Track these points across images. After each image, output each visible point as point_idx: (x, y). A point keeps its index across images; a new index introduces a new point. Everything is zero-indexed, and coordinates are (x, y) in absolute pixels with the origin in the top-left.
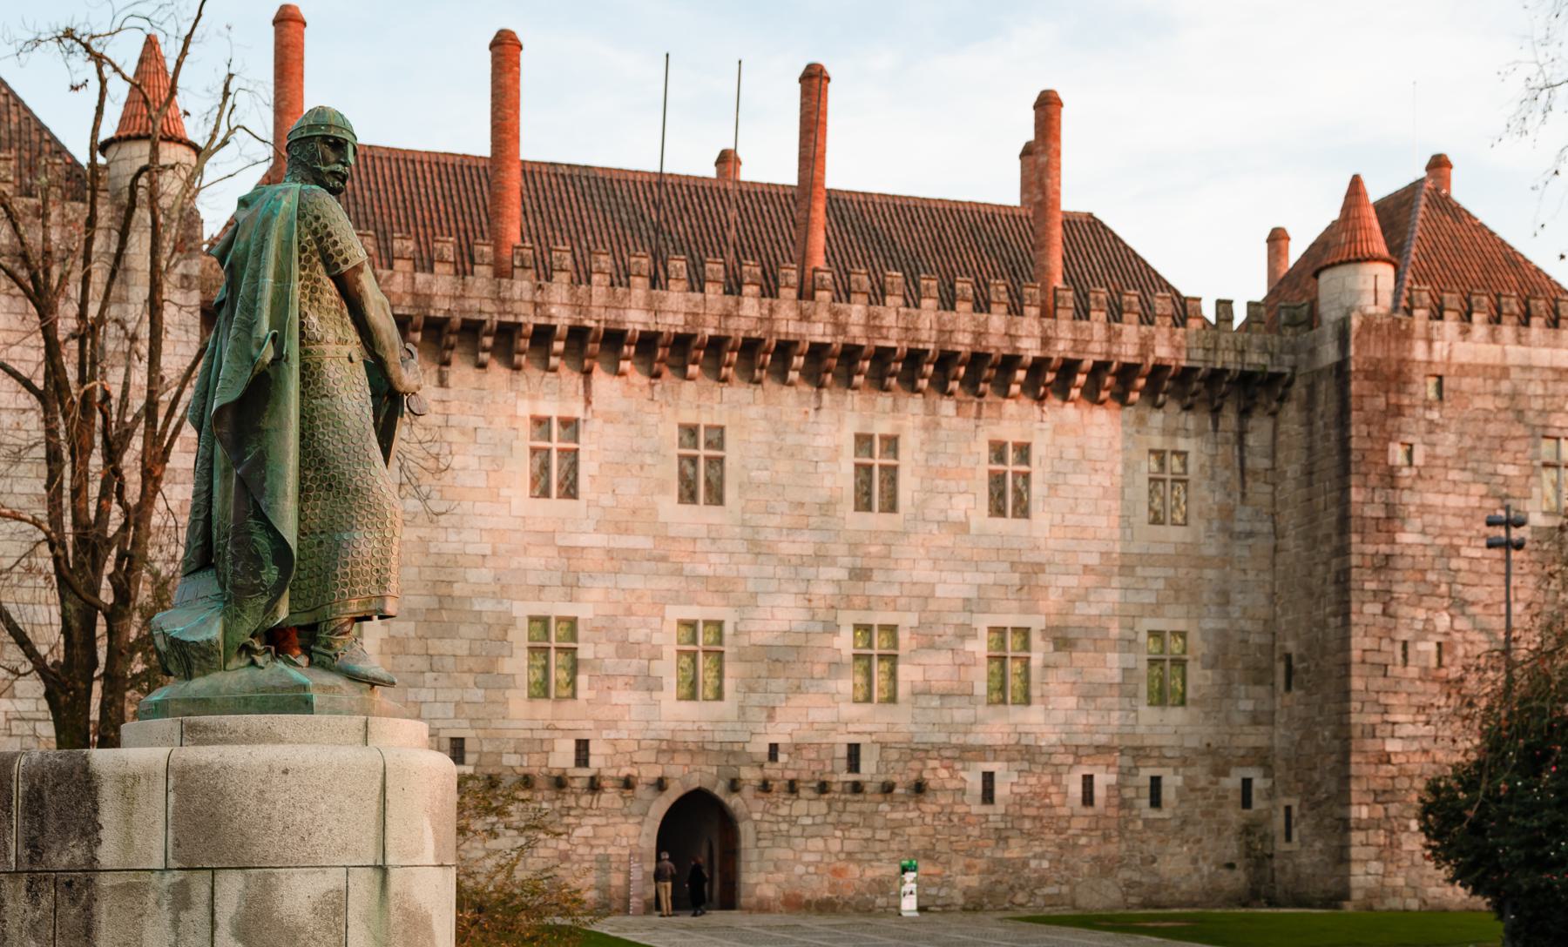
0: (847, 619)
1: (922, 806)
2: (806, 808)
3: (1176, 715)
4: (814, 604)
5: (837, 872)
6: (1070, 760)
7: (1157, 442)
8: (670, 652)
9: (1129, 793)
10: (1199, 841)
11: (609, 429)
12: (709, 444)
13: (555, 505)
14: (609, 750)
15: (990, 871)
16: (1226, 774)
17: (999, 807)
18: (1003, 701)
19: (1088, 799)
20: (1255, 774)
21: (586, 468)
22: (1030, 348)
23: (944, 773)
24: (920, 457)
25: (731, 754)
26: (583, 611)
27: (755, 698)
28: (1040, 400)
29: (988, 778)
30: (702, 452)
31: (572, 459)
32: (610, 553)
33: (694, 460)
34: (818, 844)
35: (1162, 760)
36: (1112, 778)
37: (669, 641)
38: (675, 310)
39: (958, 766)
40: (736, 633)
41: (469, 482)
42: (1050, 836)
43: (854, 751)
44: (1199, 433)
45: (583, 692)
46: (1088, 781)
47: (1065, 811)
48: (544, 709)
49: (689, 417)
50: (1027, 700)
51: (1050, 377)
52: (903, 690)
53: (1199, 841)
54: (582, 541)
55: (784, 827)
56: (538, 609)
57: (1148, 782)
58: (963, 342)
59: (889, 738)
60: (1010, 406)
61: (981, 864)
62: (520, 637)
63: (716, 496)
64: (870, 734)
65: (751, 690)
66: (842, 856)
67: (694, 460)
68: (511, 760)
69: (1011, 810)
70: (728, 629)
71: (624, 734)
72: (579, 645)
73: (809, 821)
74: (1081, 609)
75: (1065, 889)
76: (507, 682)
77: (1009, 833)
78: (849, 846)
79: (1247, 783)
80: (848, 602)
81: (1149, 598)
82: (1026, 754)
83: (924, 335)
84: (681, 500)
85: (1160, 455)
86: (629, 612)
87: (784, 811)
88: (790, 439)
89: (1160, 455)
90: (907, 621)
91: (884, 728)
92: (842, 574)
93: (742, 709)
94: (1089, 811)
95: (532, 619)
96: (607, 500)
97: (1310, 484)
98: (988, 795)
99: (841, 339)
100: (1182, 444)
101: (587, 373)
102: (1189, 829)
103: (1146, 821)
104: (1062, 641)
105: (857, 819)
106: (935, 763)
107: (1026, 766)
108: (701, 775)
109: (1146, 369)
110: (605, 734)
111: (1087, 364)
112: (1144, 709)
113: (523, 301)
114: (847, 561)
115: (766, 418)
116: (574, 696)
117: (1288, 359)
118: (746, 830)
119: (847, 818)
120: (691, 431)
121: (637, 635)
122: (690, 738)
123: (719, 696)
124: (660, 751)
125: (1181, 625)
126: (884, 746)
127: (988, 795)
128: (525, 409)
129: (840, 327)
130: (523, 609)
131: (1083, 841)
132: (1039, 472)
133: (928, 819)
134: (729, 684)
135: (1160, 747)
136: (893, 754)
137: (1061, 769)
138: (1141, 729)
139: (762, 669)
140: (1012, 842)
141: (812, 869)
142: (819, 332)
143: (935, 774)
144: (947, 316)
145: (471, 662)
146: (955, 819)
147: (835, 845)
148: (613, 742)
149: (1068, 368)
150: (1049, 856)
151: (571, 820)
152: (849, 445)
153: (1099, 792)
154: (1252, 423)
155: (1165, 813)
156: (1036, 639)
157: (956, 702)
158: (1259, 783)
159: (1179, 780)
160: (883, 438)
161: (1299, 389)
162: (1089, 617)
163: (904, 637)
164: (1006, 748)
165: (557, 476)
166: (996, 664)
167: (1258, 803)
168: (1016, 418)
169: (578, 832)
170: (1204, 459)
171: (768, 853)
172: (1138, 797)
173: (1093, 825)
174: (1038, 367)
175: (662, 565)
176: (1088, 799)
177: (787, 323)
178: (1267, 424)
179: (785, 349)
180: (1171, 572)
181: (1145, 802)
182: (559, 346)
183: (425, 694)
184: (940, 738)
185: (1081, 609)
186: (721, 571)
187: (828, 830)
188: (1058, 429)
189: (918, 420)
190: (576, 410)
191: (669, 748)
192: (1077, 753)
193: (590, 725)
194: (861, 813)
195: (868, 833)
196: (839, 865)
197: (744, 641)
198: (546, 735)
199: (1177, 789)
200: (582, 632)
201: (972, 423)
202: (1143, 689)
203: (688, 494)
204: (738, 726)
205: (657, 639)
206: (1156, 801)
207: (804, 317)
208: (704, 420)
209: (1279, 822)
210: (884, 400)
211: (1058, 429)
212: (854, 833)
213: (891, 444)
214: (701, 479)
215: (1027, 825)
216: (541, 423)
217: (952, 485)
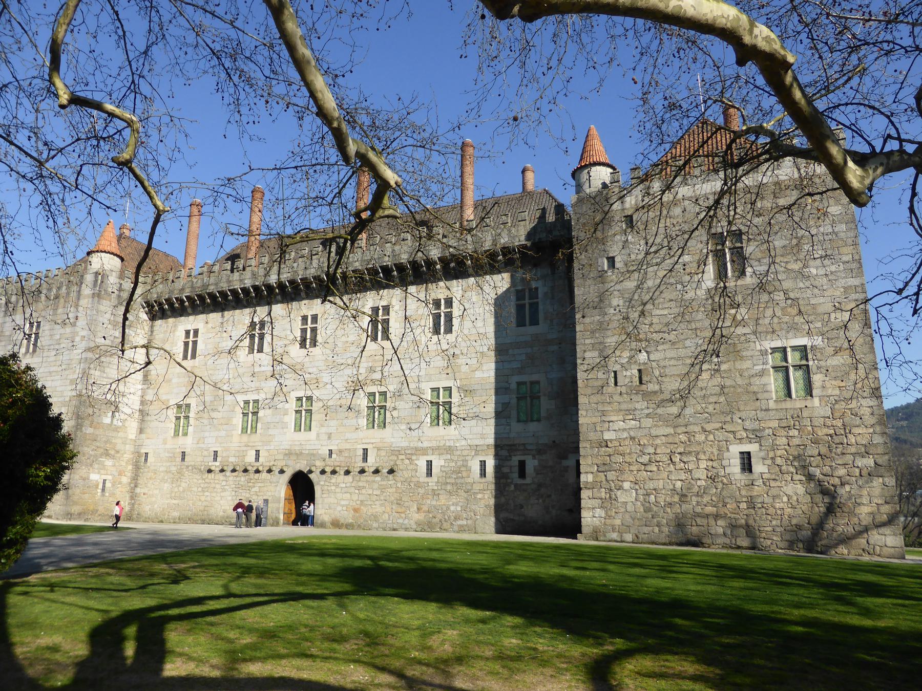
1: (397, 479)
3: (533, 427)
5: (356, 510)
6: (473, 453)
9: (505, 470)
10: (549, 496)
14: (267, 454)
15: (428, 512)
16: (566, 458)
17: (434, 478)
19: (483, 473)
23: (407, 462)
25: (313, 455)
27: (323, 430)
29: (429, 464)
34: (348, 495)
35: (526, 451)
39: (414, 457)
42: (462, 493)
43: (365, 451)
47: (470, 480)
48: (245, 438)
53: (549, 496)
55: (333, 488)
57: (517, 463)
59: (381, 445)
61: (425, 508)
65: (322, 426)
66: (358, 502)
68: (232, 459)
69: (440, 480)
71: (272, 447)
73: (344, 485)
75: (469, 522)
77: (440, 492)
78: (362, 498)
81: (516, 365)
87: (333, 481)
91: (378, 440)
93: (318, 435)
94: (484, 480)
98: (429, 473)
102: (543, 490)
103: (516, 485)
104: (467, 391)
105: (365, 484)
106: (403, 457)
107: (449, 456)
108: (303, 466)
110: (265, 448)
112: (514, 424)
118: (317, 489)
119: (361, 484)
122: (297, 448)
125: (535, 377)
126: (379, 449)
127: (429, 473)
131: (479, 496)
132: (456, 311)
133: (399, 485)
135: (524, 444)
136: (383, 453)
137: (469, 458)
138: (512, 435)
141: (344, 508)
143: (402, 464)
146: (412, 485)
147: (355, 497)
148: (268, 451)
150: (461, 504)
155: (528, 480)
159: (536, 462)
162: (482, 378)
164: (438, 448)
166: (435, 408)
168: (439, 290)
169: (254, 490)
171: (326, 501)
172: (511, 472)
173: (486, 488)
176: (483, 473)
180: (529, 350)
181: (516, 475)
183: (207, 434)
187: (352, 490)
189: (399, 298)
191: (289, 454)
192: (476, 449)
194: (367, 481)
195: (370, 492)
198: (245, 448)
199: (535, 467)
202: (514, 413)
204: (316, 442)
206: (522, 474)
208: (309, 314)
212: (364, 491)
215: (449, 487)
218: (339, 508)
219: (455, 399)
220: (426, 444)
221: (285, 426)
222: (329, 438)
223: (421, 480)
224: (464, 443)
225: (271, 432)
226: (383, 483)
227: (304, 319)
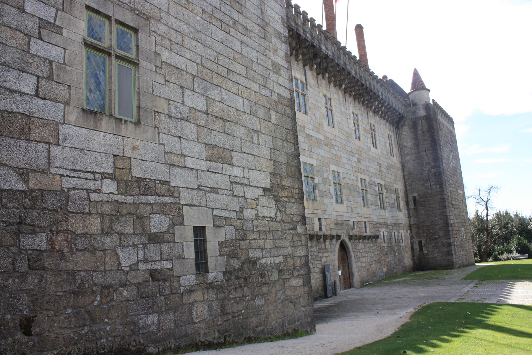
2: (361, 246)
4: (354, 170)
40: (343, 178)
45: (318, 199)
52: (369, 202)
55: (358, 253)
64: (367, 218)
70: (341, 176)
72: (315, 177)
90: (367, 179)
92: (356, 160)
96: (314, 119)
97: (418, 149)
119: (368, 249)
121: (326, 175)
124: (335, 224)
134: (344, 197)
138: (398, 218)
140: (389, 255)
151: (321, 255)
161: (408, 122)
163: (367, 183)
193: (320, 212)
196: (368, 267)
218: (362, 270)
220: (381, 221)
226: (373, 248)
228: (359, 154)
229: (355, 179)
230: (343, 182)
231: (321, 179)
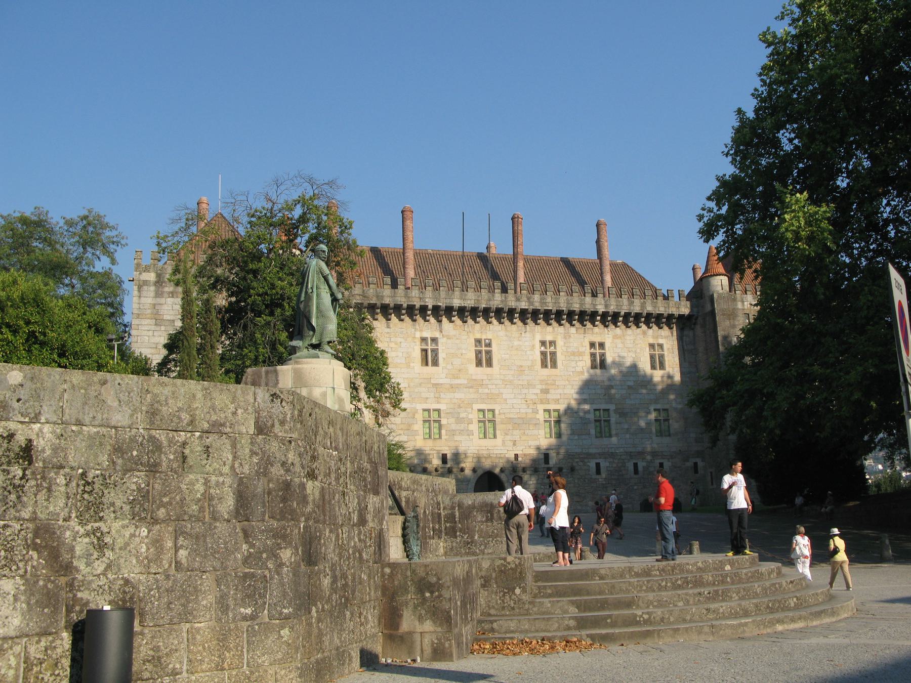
0: (541, 408)
3: (666, 440)
7: (651, 341)
8: (475, 421)
9: (652, 469)
11: (449, 341)
12: (486, 346)
13: (430, 369)
17: (604, 475)
18: (601, 437)
20: (699, 461)
21: (441, 356)
22: (601, 309)
23: (581, 464)
24: (564, 349)
26: (442, 407)
27: (508, 437)
28: (606, 326)
29: (598, 465)
30: (484, 348)
31: (435, 352)
32: (452, 386)
33: (480, 352)
36: (644, 464)
37: (475, 416)
38: (470, 300)
41: (399, 361)
44: (666, 337)
46: (636, 465)
49: (478, 336)
50: (610, 436)
51: (609, 318)
54: (441, 381)
56: (426, 406)
58: (576, 307)
60: (596, 329)
62: (420, 417)
63: (489, 364)
65: (507, 434)
67: (480, 352)
70: (497, 412)
74: (628, 401)
76: (416, 433)
79: (696, 464)
80: (542, 403)
82: (611, 455)
83: (562, 305)
84: (477, 366)
85: (652, 346)
86: (460, 407)
88: (516, 343)
89: (652, 346)
95: (424, 410)
96: (450, 367)
98: (598, 471)
99: (532, 307)
100: (661, 341)
101: (440, 321)
109: (644, 314)
111: (622, 313)
112: (654, 438)
113: (415, 298)
114: (540, 387)
115: (506, 336)
116: (440, 437)
117: (695, 310)
120: (478, 342)
121: (463, 415)
122: (484, 452)
123: (495, 437)
127: (598, 471)
128: (418, 335)
129: (531, 303)
130: (420, 407)
134: (498, 432)
139: (510, 427)
142: (524, 305)
144: (570, 298)
145: (402, 426)
149: (616, 315)
152: (538, 344)
153: (640, 469)
154: (686, 333)
156: (612, 413)
157: (584, 437)
158: (701, 464)
160: (551, 343)
161: (700, 320)
165: (429, 357)
166: (598, 424)
167: (701, 471)
170: (669, 346)
174: (605, 315)
175: (471, 390)
177: (511, 302)
178: (691, 333)
179: (511, 313)
182: (429, 312)
184: (580, 451)
185: (628, 401)
186: (493, 391)
188: (615, 337)
190: (437, 334)
192: (631, 455)
197: (503, 416)
200: (442, 415)
201: (582, 336)
203: (479, 363)
205: (470, 416)
207: (518, 300)
208: (484, 337)
209: (709, 478)
210: (549, 328)
211: (615, 337)
213: (553, 343)
214: (484, 358)
216: (424, 340)
217: (577, 358)
219: (614, 418)
221: (470, 433)
222: (514, 444)
223: (594, 477)
224: (622, 450)
225: (457, 438)
227: (478, 342)
228: (547, 384)
229: (531, 411)
230: (497, 420)
231: (453, 420)
